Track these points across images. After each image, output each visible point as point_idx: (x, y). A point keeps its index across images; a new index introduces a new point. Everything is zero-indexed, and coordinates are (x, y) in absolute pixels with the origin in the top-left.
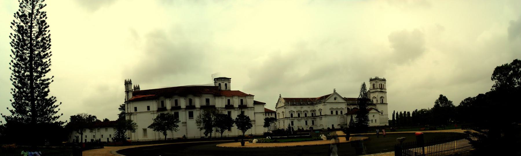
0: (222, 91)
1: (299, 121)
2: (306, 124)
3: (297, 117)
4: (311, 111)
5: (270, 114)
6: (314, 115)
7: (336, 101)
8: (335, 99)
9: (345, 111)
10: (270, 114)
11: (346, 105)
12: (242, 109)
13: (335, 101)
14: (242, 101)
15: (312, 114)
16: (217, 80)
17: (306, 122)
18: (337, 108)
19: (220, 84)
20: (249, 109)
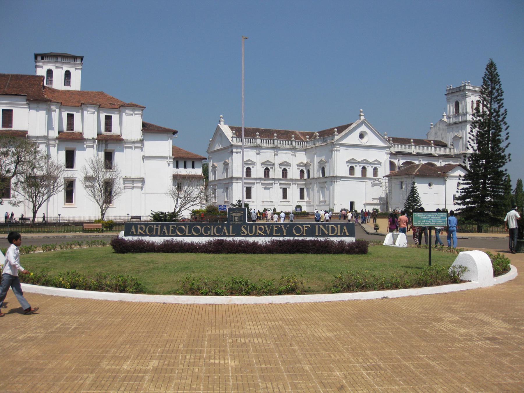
0: (54, 91)
1: (266, 188)
2: (285, 196)
3: (260, 179)
4: (297, 165)
5: (189, 164)
6: (306, 176)
7: (364, 141)
8: (362, 136)
9: (384, 170)
10: (189, 164)
11: (387, 153)
12: (107, 145)
13: (362, 141)
14: (108, 119)
15: (302, 172)
16: (43, 59)
17: (285, 191)
18: (365, 160)
19: (50, 73)
20: (127, 145)
